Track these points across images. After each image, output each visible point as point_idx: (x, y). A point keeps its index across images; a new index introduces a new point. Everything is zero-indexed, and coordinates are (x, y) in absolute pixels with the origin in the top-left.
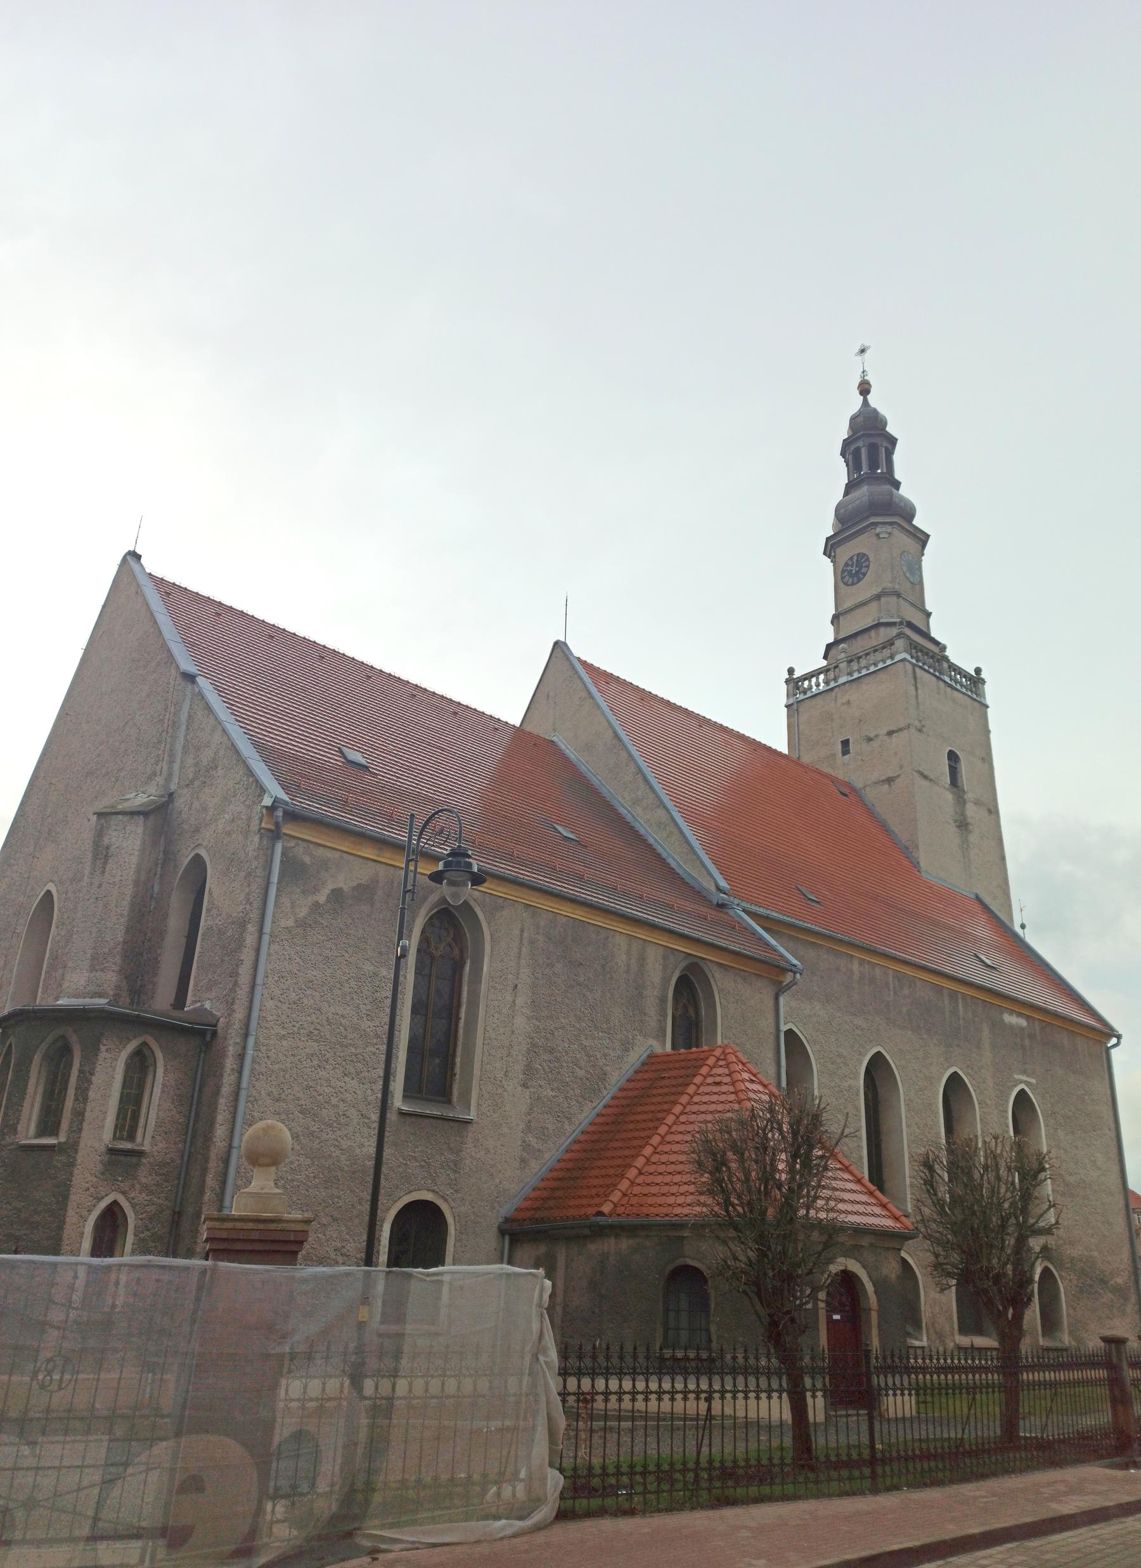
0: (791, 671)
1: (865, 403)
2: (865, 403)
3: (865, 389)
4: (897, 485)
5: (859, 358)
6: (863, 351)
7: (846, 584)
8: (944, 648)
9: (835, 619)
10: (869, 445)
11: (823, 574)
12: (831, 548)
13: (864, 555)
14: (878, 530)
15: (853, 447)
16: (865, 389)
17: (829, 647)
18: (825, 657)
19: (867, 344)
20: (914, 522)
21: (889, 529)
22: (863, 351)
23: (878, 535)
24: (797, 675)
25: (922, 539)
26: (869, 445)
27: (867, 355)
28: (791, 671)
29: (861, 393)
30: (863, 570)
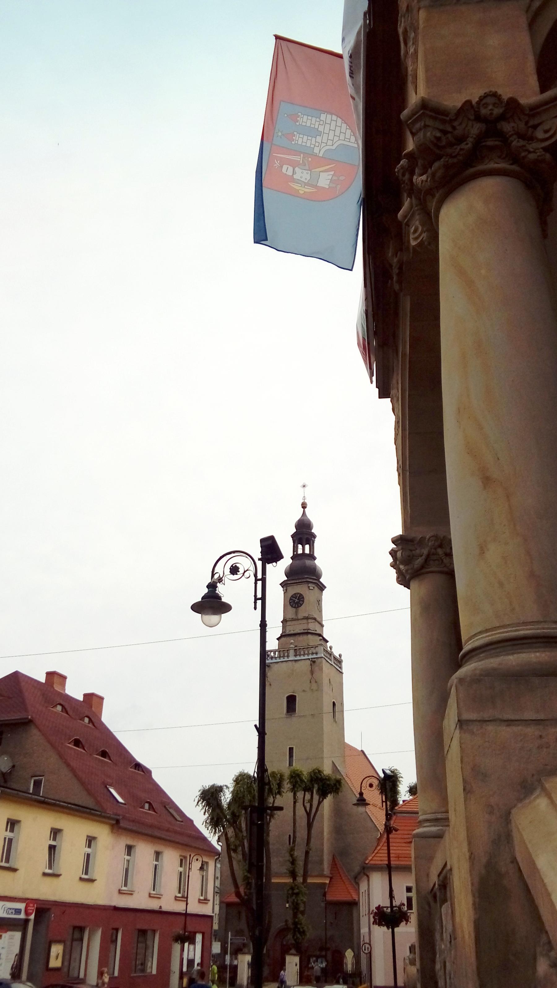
3: (304, 506)
4: (314, 558)
5: (302, 489)
6: (304, 486)
7: (292, 606)
13: (301, 595)
14: (310, 585)
15: (299, 537)
16: (304, 506)
19: (307, 483)
20: (321, 580)
21: (314, 586)
22: (304, 486)
25: (322, 588)
27: (306, 488)
29: (303, 507)
30: (301, 602)
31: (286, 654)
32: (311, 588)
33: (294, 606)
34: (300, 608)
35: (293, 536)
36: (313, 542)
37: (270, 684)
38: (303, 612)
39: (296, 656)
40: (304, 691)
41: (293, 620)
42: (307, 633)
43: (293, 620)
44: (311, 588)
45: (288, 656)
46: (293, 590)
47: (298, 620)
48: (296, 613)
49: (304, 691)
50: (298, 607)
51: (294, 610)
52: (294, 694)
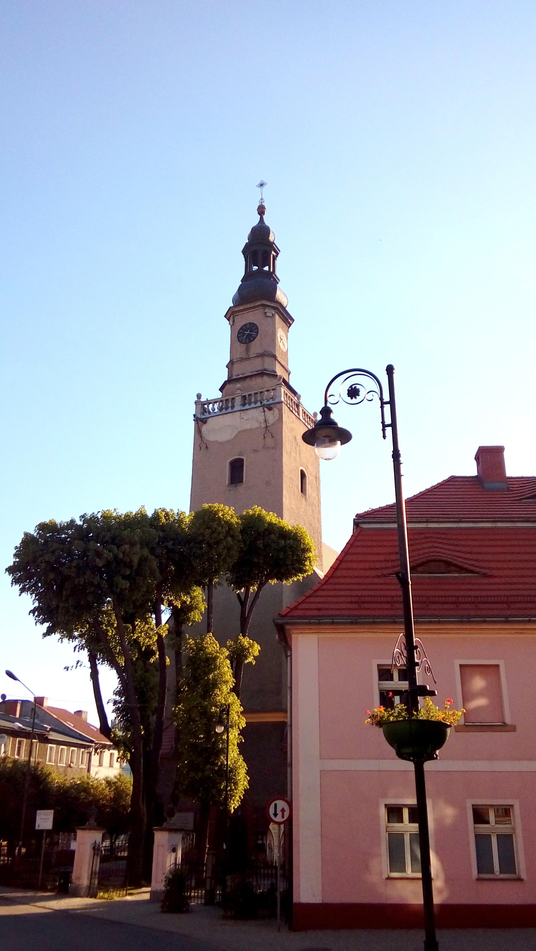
0: (199, 396)
1: (262, 219)
2: (262, 219)
3: (261, 210)
6: (262, 185)
7: (241, 342)
8: (299, 398)
9: (230, 366)
10: (260, 249)
11: (224, 332)
12: (230, 315)
13: (254, 324)
14: (266, 310)
16: (261, 210)
17: (225, 383)
18: (221, 389)
19: (265, 181)
22: (262, 185)
23: (266, 313)
24: (203, 399)
26: (260, 249)
27: (265, 188)
28: (199, 396)
29: (259, 214)
31: (230, 405)
32: (268, 314)
33: (244, 341)
34: (252, 343)
35: (244, 252)
36: (275, 258)
37: (207, 447)
38: (256, 347)
39: (244, 405)
40: (255, 451)
41: (242, 360)
42: (262, 373)
43: (242, 360)
44: (268, 314)
45: (233, 407)
46: (241, 321)
47: (248, 359)
48: (247, 350)
49: (255, 451)
50: (251, 341)
51: (244, 346)
52: (241, 457)
